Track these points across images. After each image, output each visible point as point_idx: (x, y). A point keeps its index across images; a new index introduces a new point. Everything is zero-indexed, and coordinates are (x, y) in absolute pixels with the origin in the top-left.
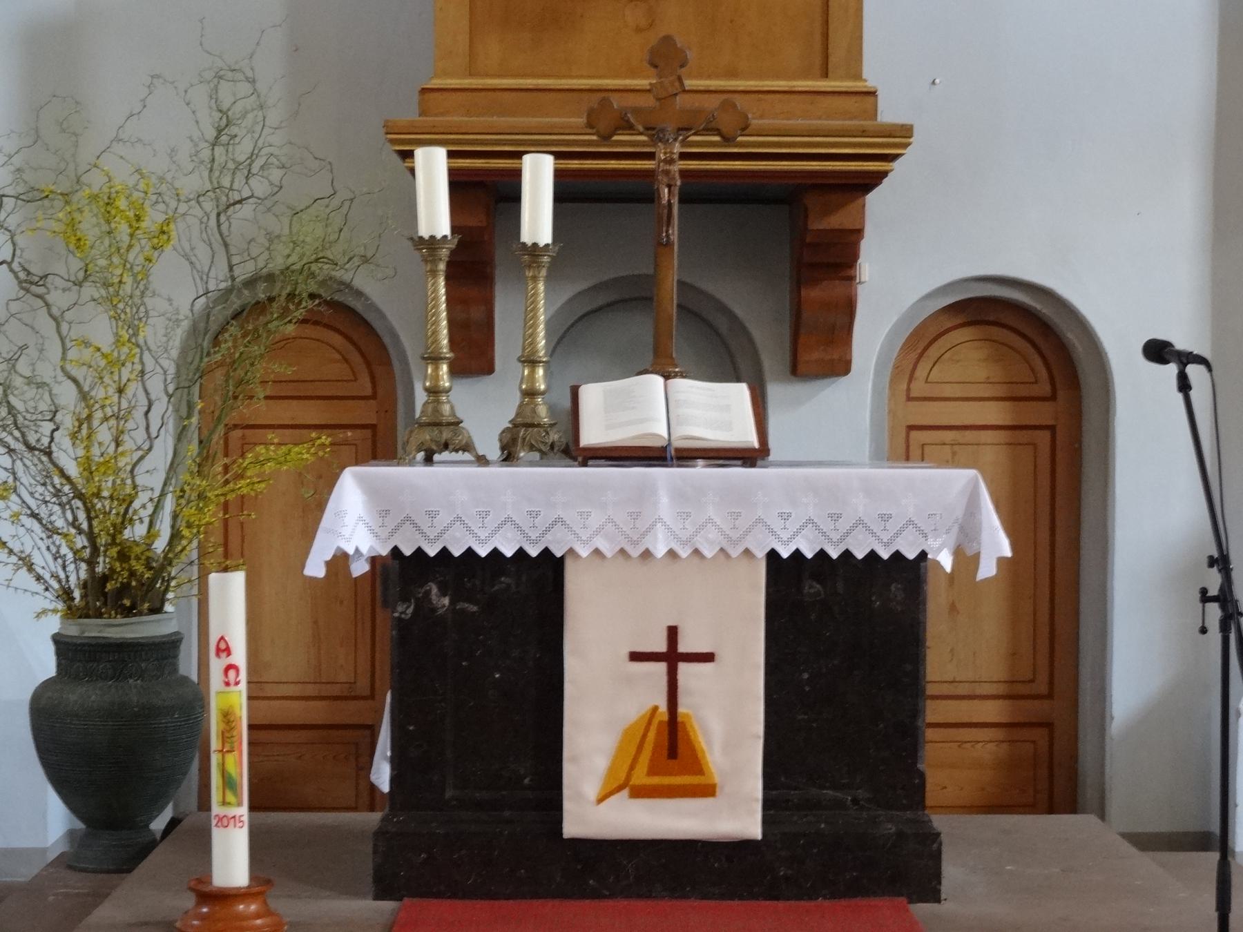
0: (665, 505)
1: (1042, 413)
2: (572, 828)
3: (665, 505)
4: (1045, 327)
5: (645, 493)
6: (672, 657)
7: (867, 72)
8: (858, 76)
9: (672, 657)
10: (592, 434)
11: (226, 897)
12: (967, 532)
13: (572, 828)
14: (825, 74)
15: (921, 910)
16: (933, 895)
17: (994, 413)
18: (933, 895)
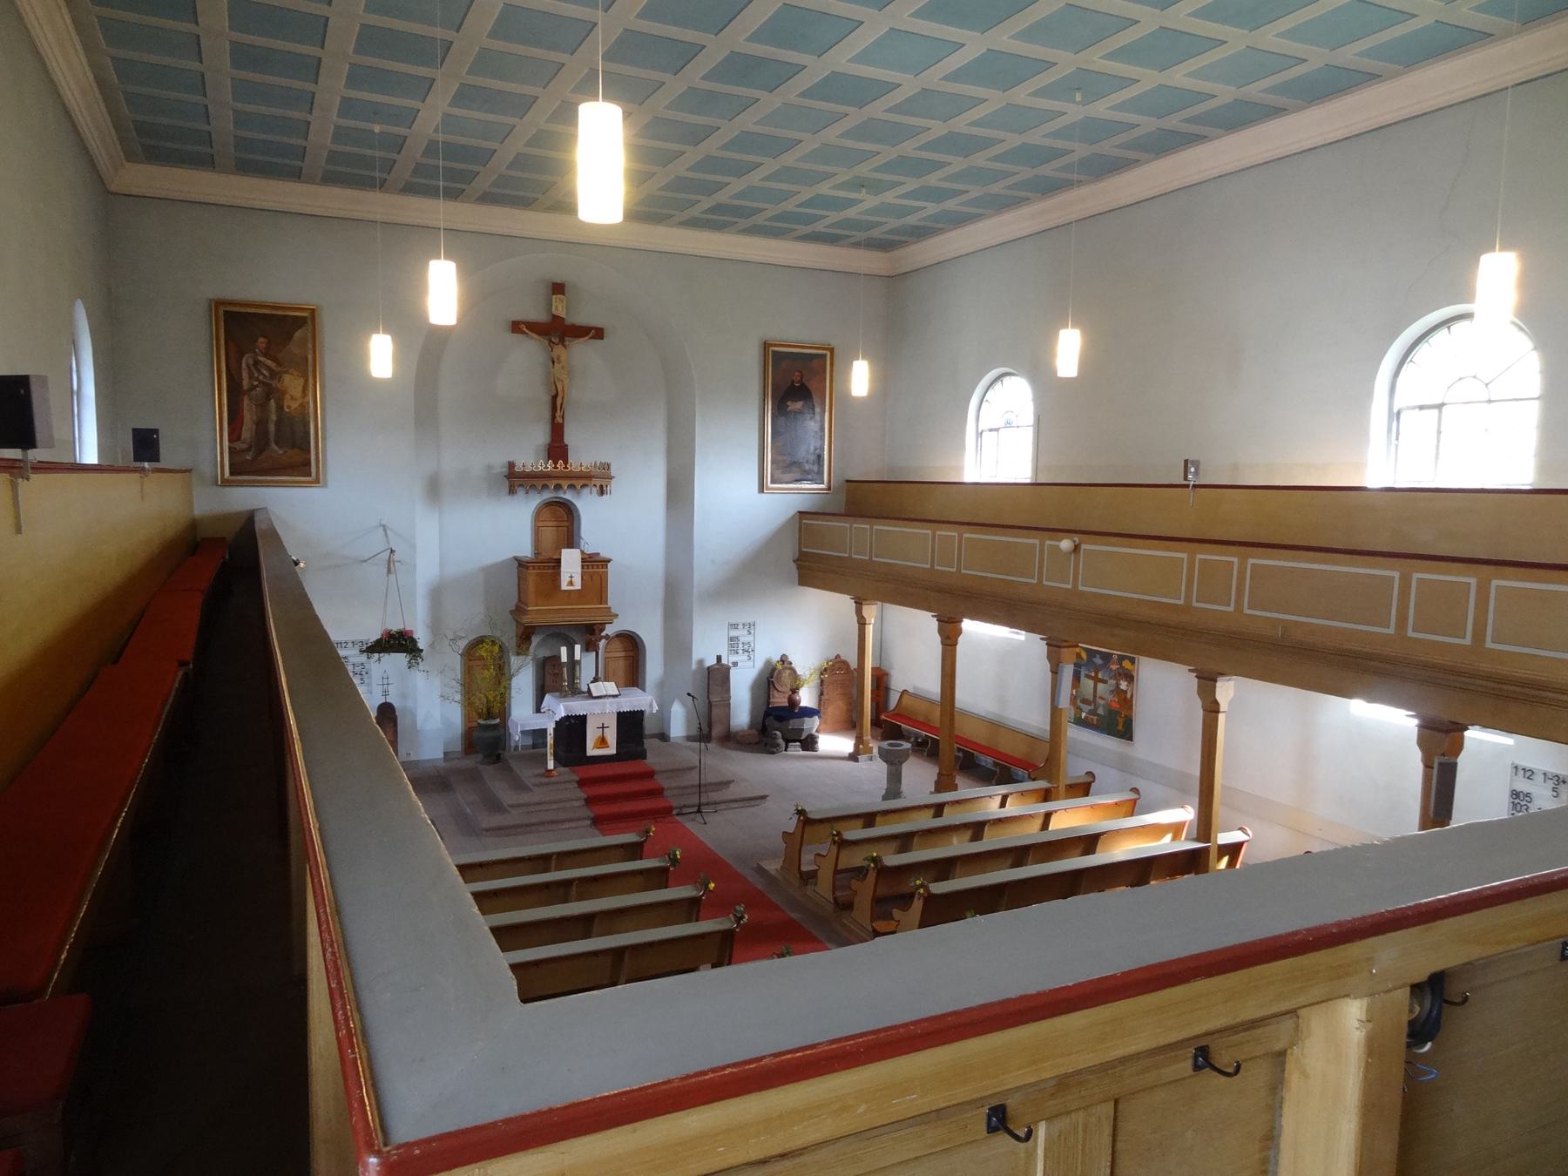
0: (608, 706)
1: (631, 654)
2: (588, 754)
3: (608, 706)
4: (632, 637)
5: (605, 703)
6: (603, 728)
7: (609, 603)
8: (607, 604)
9: (603, 728)
10: (595, 694)
11: (551, 771)
12: (651, 705)
13: (588, 754)
14: (601, 604)
15: (645, 761)
16: (646, 759)
17: (623, 654)
18: (646, 759)
